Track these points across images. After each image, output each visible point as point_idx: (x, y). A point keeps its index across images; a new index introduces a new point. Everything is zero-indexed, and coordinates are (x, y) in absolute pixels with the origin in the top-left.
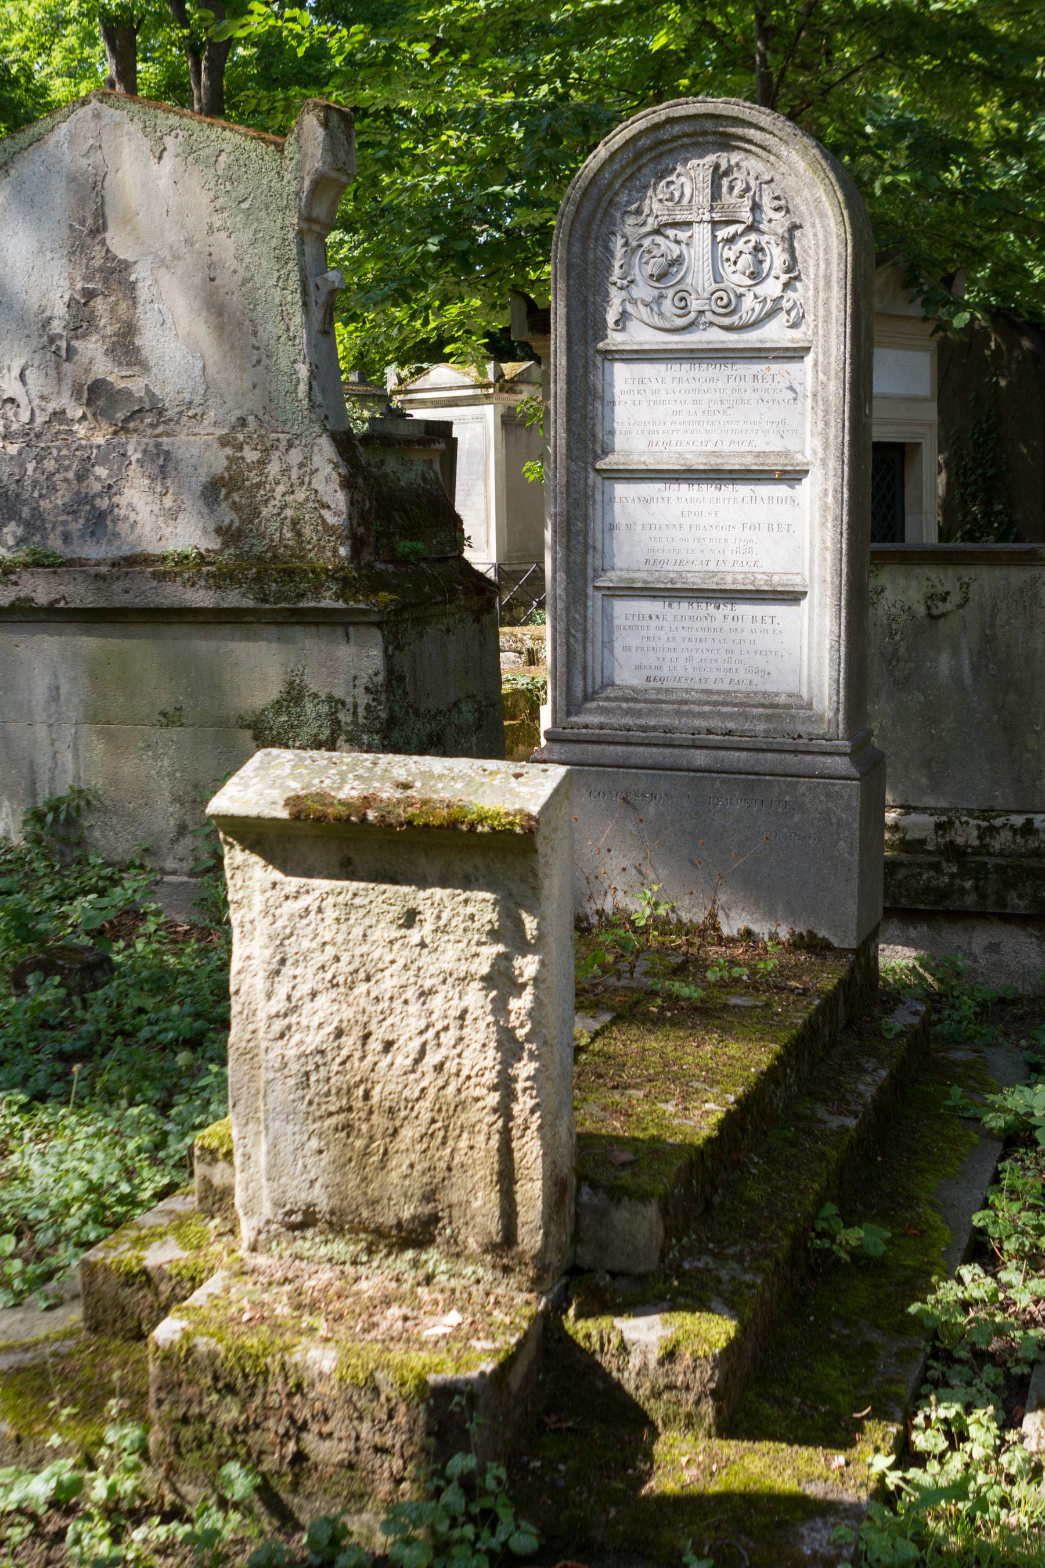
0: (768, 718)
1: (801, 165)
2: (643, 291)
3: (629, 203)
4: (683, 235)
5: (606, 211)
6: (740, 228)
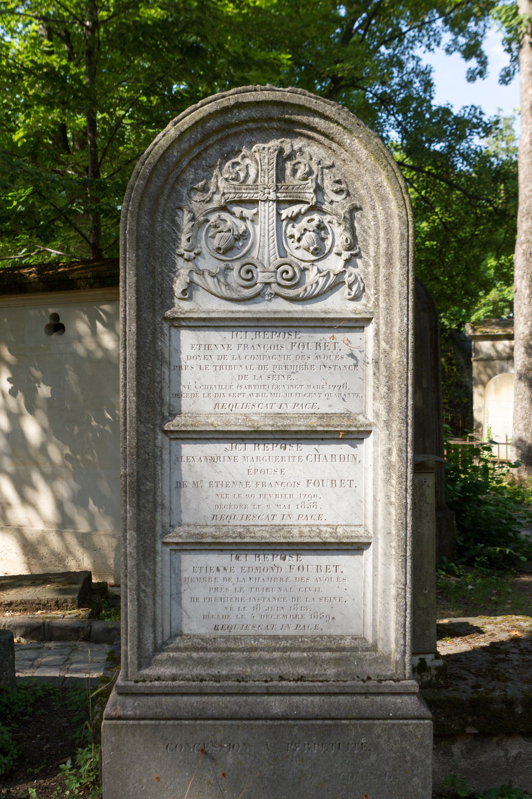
0: (337, 662)
1: (363, 153)
2: (209, 263)
3: (196, 180)
4: (248, 213)
5: (173, 187)
6: (304, 208)
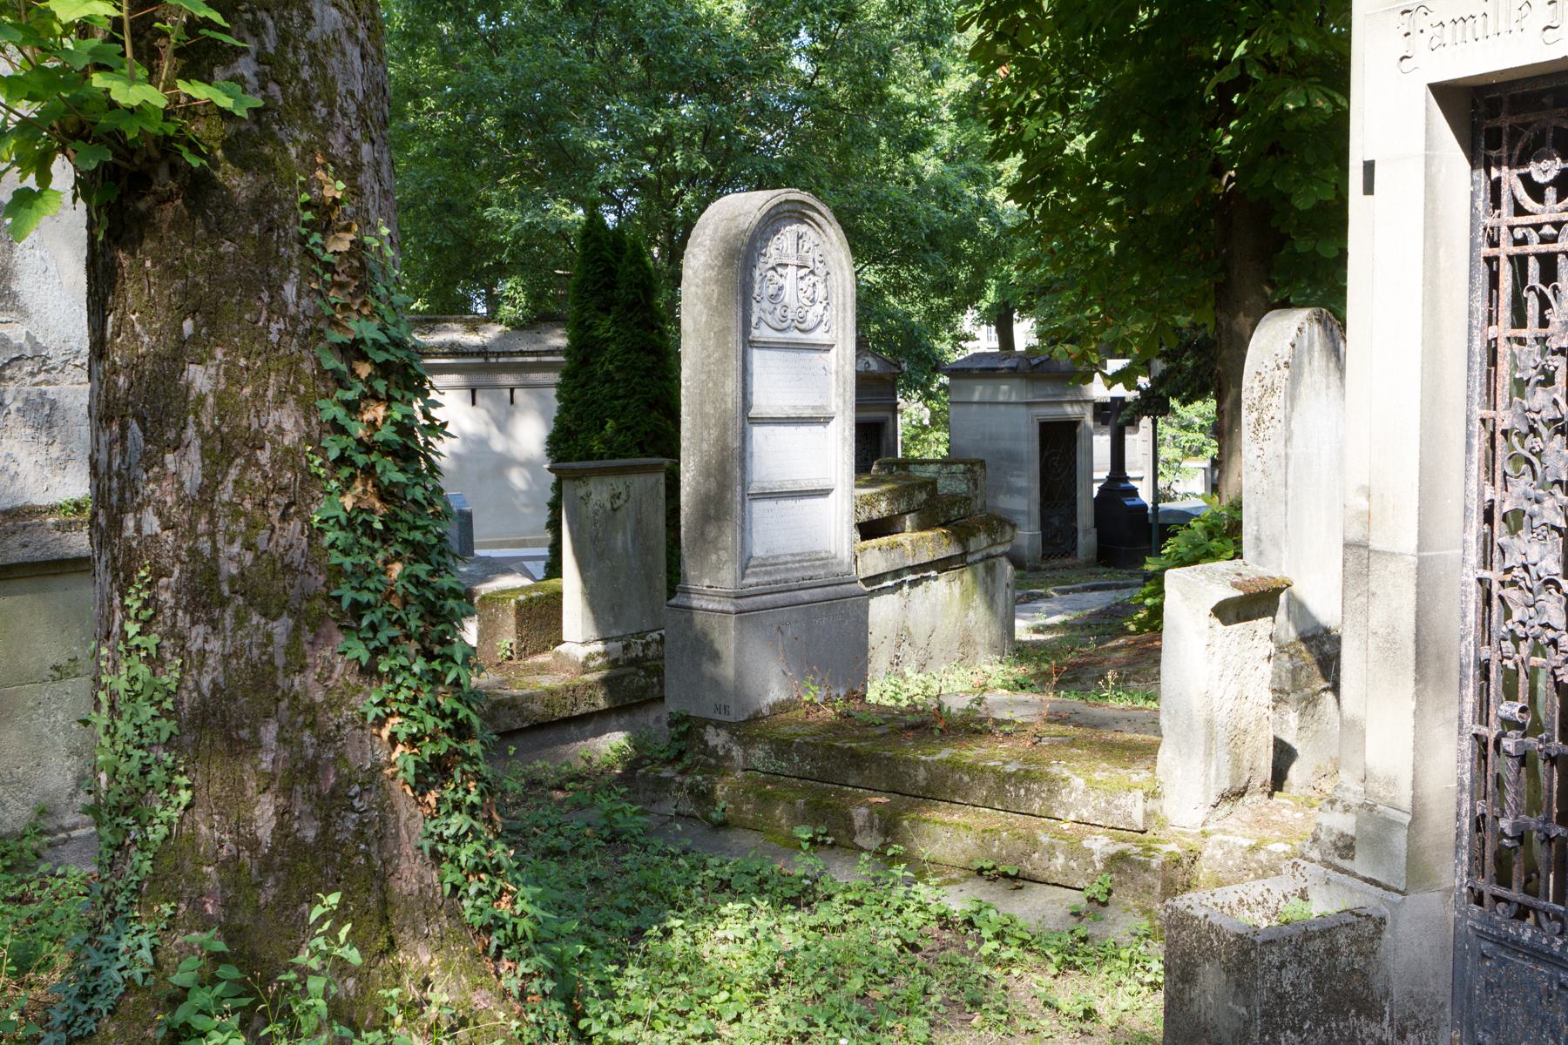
0: (823, 566)
1: (834, 238)
